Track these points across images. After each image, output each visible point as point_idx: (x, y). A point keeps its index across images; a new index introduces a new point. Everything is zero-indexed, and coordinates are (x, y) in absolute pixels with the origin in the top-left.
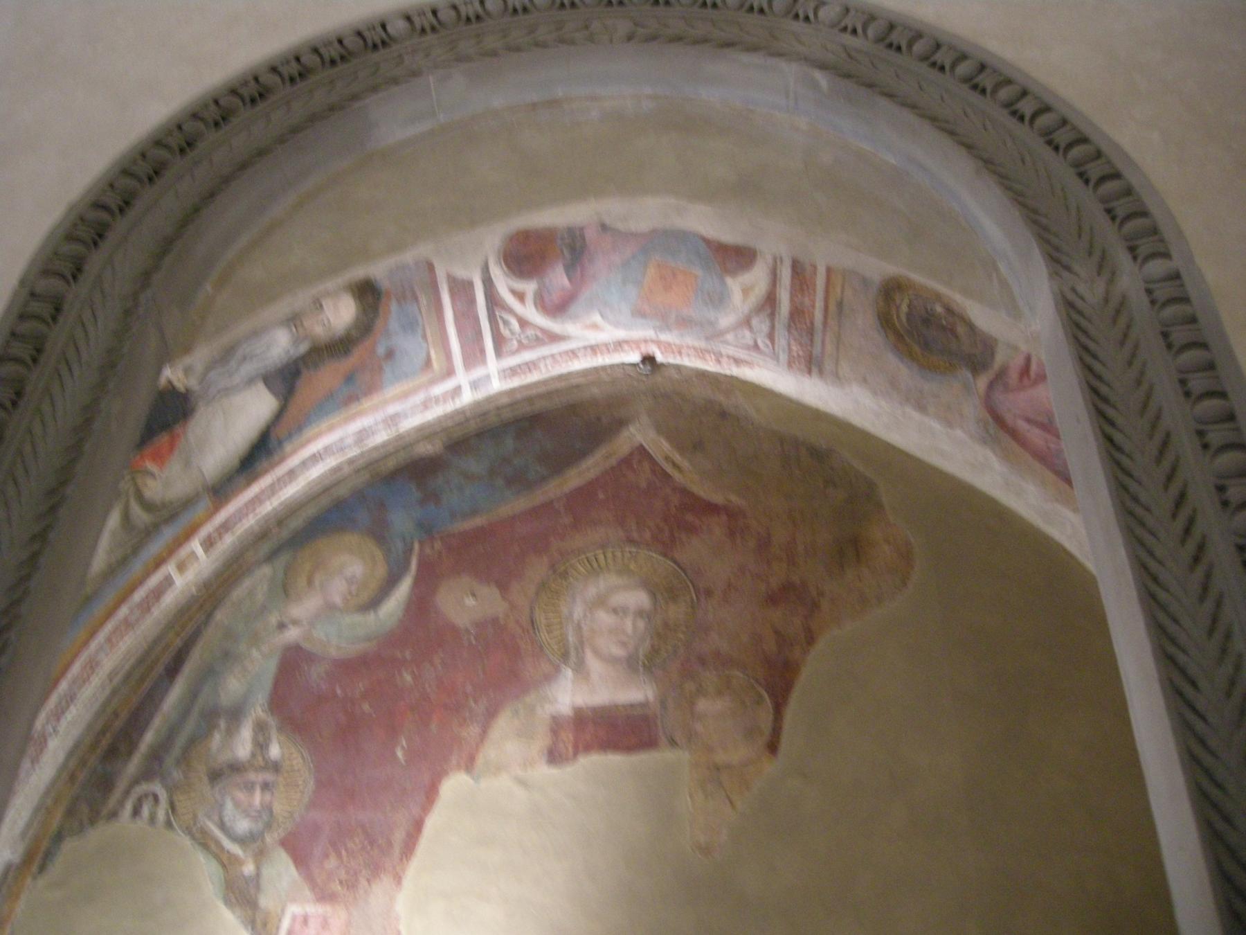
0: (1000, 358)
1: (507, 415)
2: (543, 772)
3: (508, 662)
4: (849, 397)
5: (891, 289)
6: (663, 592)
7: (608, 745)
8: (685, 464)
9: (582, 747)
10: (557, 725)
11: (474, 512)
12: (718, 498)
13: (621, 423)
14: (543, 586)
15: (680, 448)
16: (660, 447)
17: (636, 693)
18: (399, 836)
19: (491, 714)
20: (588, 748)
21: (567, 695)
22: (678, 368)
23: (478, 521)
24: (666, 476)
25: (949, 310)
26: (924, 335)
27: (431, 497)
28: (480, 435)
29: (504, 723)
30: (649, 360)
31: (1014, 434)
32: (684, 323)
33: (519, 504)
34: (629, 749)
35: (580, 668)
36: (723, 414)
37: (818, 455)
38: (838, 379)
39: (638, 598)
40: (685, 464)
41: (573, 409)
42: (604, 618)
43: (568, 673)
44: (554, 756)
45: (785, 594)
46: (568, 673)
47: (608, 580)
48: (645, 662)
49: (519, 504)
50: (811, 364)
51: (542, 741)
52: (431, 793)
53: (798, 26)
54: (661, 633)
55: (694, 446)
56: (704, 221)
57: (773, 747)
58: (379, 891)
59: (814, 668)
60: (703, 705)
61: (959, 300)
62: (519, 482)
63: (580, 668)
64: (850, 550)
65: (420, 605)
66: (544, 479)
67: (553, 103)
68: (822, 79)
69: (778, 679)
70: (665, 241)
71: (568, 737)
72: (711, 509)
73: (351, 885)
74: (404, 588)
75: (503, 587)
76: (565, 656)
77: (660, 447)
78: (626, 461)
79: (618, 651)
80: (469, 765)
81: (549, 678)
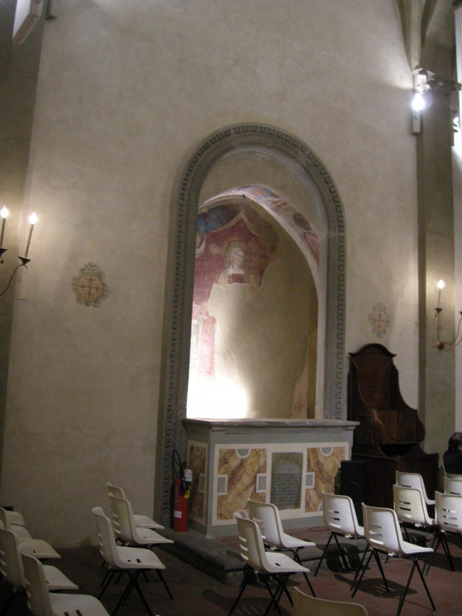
0: (311, 231)
1: (219, 205)
2: (228, 285)
3: (221, 263)
5: (299, 214)
6: (246, 253)
7: (237, 281)
8: (249, 224)
9: (234, 281)
10: (230, 276)
11: (214, 229)
12: (254, 233)
13: (239, 211)
14: (227, 248)
15: (249, 220)
16: (245, 219)
17: (241, 272)
18: (207, 294)
19: (220, 273)
20: (234, 282)
21: (231, 271)
22: (249, 199)
23: (215, 231)
24: (246, 226)
25: (307, 222)
26: (299, 221)
27: (207, 224)
28: (214, 209)
29: (222, 275)
30: (244, 196)
32: (256, 195)
33: (222, 228)
34: (240, 282)
35: (233, 266)
36: (256, 213)
37: (271, 226)
38: (279, 214)
39: (241, 253)
40: (249, 224)
41: (230, 205)
42: (236, 256)
43: (231, 267)
44: (229, 282)
45: (264, 257)
46: (231, 267)
48: (243, 267)
49: (222, 228)
50: (275, 210)
51: (227, 279)
52: (211, 287)
53: (300, 152)
55: (251, 220)
57: (260, 285)
58: (205, 303)
60: (251, 276)
61: (309, 221)
62: (222, 223)
63: (233, 266)
64: (273, 249)
65: (207, 249)
66: (227, 223)
67: (252, 152)
68: (302, 170)
69: (261, 273)
71: (231, 279)
72: (253, 236)
73: (200, 302)
74: (204, 245)
75: (220, 247)
76: (231, 263)
77: (245, 219)
78: (240, 221)
79: (239, 264)
80: (217, 282)
81: (228, 267)
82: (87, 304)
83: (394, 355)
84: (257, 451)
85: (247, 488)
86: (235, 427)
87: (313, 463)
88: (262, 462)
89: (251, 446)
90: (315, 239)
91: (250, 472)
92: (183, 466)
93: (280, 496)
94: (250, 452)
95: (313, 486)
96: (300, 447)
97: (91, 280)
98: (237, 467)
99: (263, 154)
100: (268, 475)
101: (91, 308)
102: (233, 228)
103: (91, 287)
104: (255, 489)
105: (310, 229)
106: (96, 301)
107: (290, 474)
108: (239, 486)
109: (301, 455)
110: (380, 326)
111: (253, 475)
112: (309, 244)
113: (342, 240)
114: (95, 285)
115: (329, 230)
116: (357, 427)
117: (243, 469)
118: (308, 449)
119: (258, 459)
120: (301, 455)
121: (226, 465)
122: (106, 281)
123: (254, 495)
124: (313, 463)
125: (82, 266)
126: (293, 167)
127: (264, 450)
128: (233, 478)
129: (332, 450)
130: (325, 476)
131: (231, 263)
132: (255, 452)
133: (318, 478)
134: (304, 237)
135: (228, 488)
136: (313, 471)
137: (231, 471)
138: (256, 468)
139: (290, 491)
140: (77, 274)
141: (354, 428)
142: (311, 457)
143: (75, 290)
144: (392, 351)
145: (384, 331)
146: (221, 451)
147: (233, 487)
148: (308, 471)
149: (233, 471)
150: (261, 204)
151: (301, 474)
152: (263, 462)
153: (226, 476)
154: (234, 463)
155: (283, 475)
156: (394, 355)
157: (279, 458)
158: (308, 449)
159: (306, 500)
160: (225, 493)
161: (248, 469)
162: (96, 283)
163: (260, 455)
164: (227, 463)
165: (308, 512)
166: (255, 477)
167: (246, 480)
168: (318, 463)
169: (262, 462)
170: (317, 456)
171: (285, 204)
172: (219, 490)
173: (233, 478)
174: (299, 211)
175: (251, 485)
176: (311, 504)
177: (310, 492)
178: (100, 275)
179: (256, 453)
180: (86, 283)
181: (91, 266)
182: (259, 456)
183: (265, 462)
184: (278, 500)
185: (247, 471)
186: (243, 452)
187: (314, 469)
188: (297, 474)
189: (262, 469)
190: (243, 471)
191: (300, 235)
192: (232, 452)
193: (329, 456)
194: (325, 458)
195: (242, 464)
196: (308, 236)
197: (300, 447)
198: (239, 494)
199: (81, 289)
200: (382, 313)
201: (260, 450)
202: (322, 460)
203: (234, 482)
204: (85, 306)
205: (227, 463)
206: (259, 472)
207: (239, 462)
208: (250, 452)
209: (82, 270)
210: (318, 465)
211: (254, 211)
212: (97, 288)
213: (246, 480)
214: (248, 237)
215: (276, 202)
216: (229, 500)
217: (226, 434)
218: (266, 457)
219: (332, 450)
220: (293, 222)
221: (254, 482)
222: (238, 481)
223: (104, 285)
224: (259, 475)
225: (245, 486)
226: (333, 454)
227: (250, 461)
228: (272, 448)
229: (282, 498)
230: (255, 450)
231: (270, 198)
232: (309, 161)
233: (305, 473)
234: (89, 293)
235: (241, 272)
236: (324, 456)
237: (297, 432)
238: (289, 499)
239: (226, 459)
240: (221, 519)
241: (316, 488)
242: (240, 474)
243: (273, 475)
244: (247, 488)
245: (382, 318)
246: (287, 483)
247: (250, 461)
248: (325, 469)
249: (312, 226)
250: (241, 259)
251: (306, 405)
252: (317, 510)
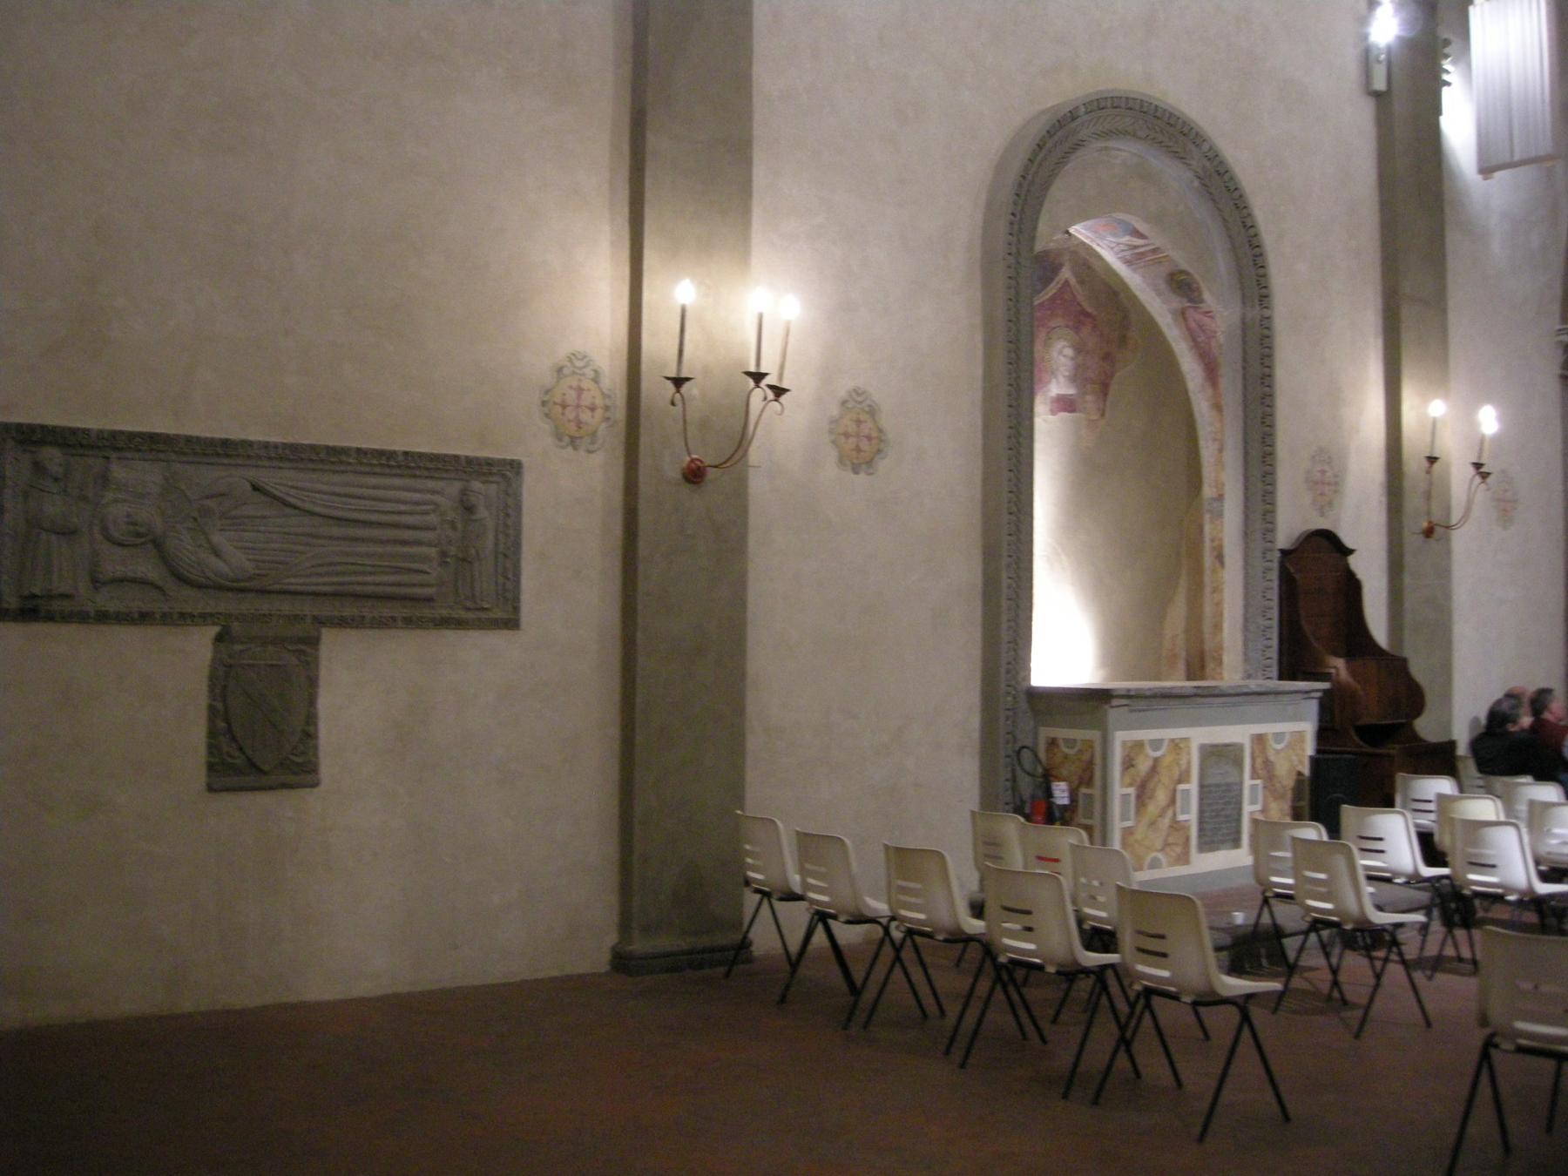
4: (1133, 279)
5: (1182, 272)
7: (1065, 410)
12: (1089, 310)
13: (1061, 266)
16: (1073, 281)
17: (1070, 391)
26: (1181, 285)
31: (1185, 319)
37: (1116, 294)
38: (1134, 270)
39: (1069, 352)
42: (1063, 359)
44: (1053, 412)
47: (1062, 343)
48: (1074, 379)
50: (1128, 262)
53: (1193, 147)
54: (1077, 367)
55: (1082, 282)
56: (1141, 227)
57: (1103, 415)
59: (1114, 388)
64: (1123, 340)
67: (1106, 148)
68: (1196, 183)
69: (1104, 389)
70: (1120, 222)
72: (1088, 315)
77: (1073, 281)
82: (856, 473)
83: (1351, 552)
86: (1146, 697)
87: (1259, 761)
88: (1183, 762)
90: (1206, 320)
92: (1047, 778)
94: (1166, 744)
96: (1238, 734)
97: (859, 422)
99: (1126, 151)
100: (1193, 787)
101: (862, 477)
102: (1053, 299)
103: (860, 438)
105: (1202, 301)
106: (870, 463)
108: (1152, 809)
110: (1322, 494)
112: (1189, 329)
113: (1266, 324)
114: (866, 432)
115: (1244, 303)
116: (1325, 691)
121: (1132, 770)
122: (886, 422)
123: (1177, 826)
125: (842, 394)
126: (1175, 176)
127: (1186, 740)
128: (1143, 793)
129: (1287, 738)
131: (1053, 374)
134: (1182, 315)
138: (1176, 773)
140: (835, 411)
141: (1319, 694)
143: (834, 442)
144: (1348, 542)
145: (1330, 504)
146: (1124, 743)
150: (1098, 249)
153: (1131, 791)
154: (1143, 766)
156: (1351, 552)
161: (1165, 778)
162: (867, 428)
166: (1175, 790)
167: (1161, 796)
168: (1268, 764)
171: (1155, 251)
172: (1124, 818)
173: (1143, 793)
174: (1184, 266)
178: (872, 412)
179: (1177, 746)
180: (852, 428)
181: (858, 394)
183: (1189, 763)
186: (1156, 744)
189: (1183, 777)
191: (1174, 313)
192: (1139, 745)
194: (1278, 752)
195: (1154, 769)
196: (1191, 314)
197: (1238, 734)
198: (1153, 824)
199: (843, 439)
200: (1326, 468)
204: (853, 476)
206: (1180, 781)
208: (1166, 744)
209: (844, 403)
211: (1087, 263)
212: (869, 438)
214: (1080, 319)
215: (1136, 247)
216: (1138, 836)
219: (1287, 738)
220: (1163, 286)
221: (1173, 801)
223: (880, 431)
226: (1290, 746)
228: (1200, 736)
231: (1126, 239)
232: (1208, 164)
233: (1248, 782)
234: (858, 449)
235: (1070, 391)
237: (1234, 705)
243: (1202, 786)
245: (1326, 481)
249: (1206, 296)
250: (1069, 363)
251: (1183, 654)
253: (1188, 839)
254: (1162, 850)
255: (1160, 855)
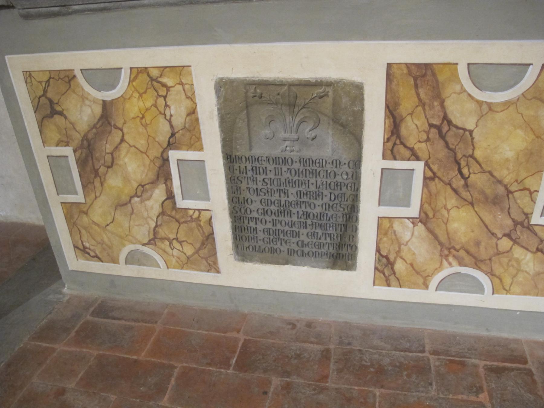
84: (155, 73)
85: (142, 190)
88: (178, 111)
89: (127, 58)
91: (142, 143)
93: (269, 226)
94: (125, 77)
95: (414, 211)
96: (359, 62)
98: (94, 126)
104: (170, 196)
107: (303, 161)
109: (356, 92)
111: (155, 152)
117: (116, 136)
118: (389, 66)
119: (161, 101)
120: (356, 92)
124: (413, 128)
127: (180, 71)
130: (477, 179)
132: (143, 77)
133: (436, 185)
135: (84, 187)
136: (418, 159)
137: (77, 137)
139: (307, 215)
142: (407, 103)
147: (97, 184)
148: (390, 153)
149: (85, 138)
151: (357, 163)
152: (184, 113)
153: (68, 151)
155: (275, 160)
157: (244, 101)
158: (389, 66)
159: (378, 250)
160: (79, 198)
161: (134, 135)
163: (168, 89)
164: (61, 113)
165: (389, 285)
166: (166, 161)
167: (135, 166)
169: (178, 111)
170: (438, 96)
175: (154, 183)
176: (399, 266)
177: (397, 226)
179: (150, 80)
182: (163, 92)
183: (192, 112)
184: (261, 235)
185: (126, 137)
186: (107, 77)
187: (422, 148)
188: (337, 163)
190: (117, 140)
192: (67, 78)
193: (507, 104)
201: (163, 69)
202: (462, 114)
203: (96, 173)
205: (61, 113)
206: (171, 145)
207: (98, 110)
208: (125, 77)
210: (442, 136)
213: (135, 166)
217: (27, 17)
218: (191, 98)
221: (163, 173)
222: (109, 167)
224: (174, 155)
225: (135, 185)
227: (134, 107)
229: (276, 232)
230: (145, 70)
236: (480, 103)
238: (303, 238)
239: (51, 101)
240: (88, 260)
241: (424, 219)
242: (109, 148)
243: (230, 159)
244: (142, 190)
246: (292, 191)
247: (134, 107)
248: (478, 154)
252: (426, 287)
253: (209, 238)
254: (152, 242)
255: (147, 250)
